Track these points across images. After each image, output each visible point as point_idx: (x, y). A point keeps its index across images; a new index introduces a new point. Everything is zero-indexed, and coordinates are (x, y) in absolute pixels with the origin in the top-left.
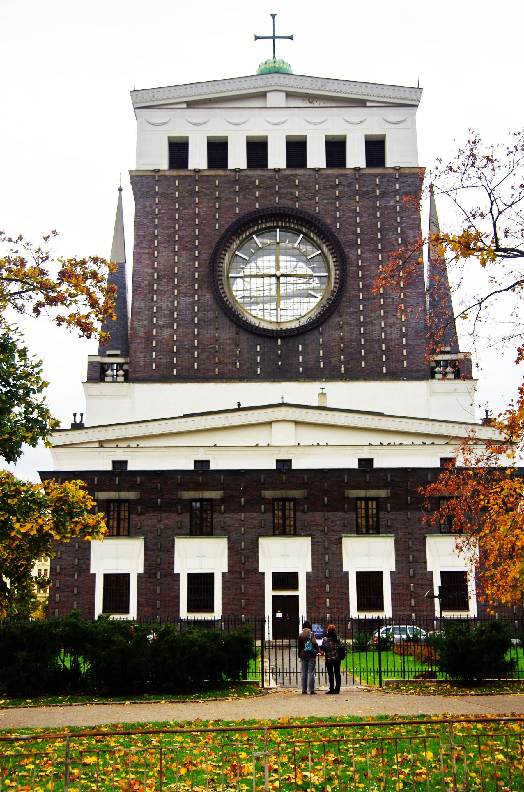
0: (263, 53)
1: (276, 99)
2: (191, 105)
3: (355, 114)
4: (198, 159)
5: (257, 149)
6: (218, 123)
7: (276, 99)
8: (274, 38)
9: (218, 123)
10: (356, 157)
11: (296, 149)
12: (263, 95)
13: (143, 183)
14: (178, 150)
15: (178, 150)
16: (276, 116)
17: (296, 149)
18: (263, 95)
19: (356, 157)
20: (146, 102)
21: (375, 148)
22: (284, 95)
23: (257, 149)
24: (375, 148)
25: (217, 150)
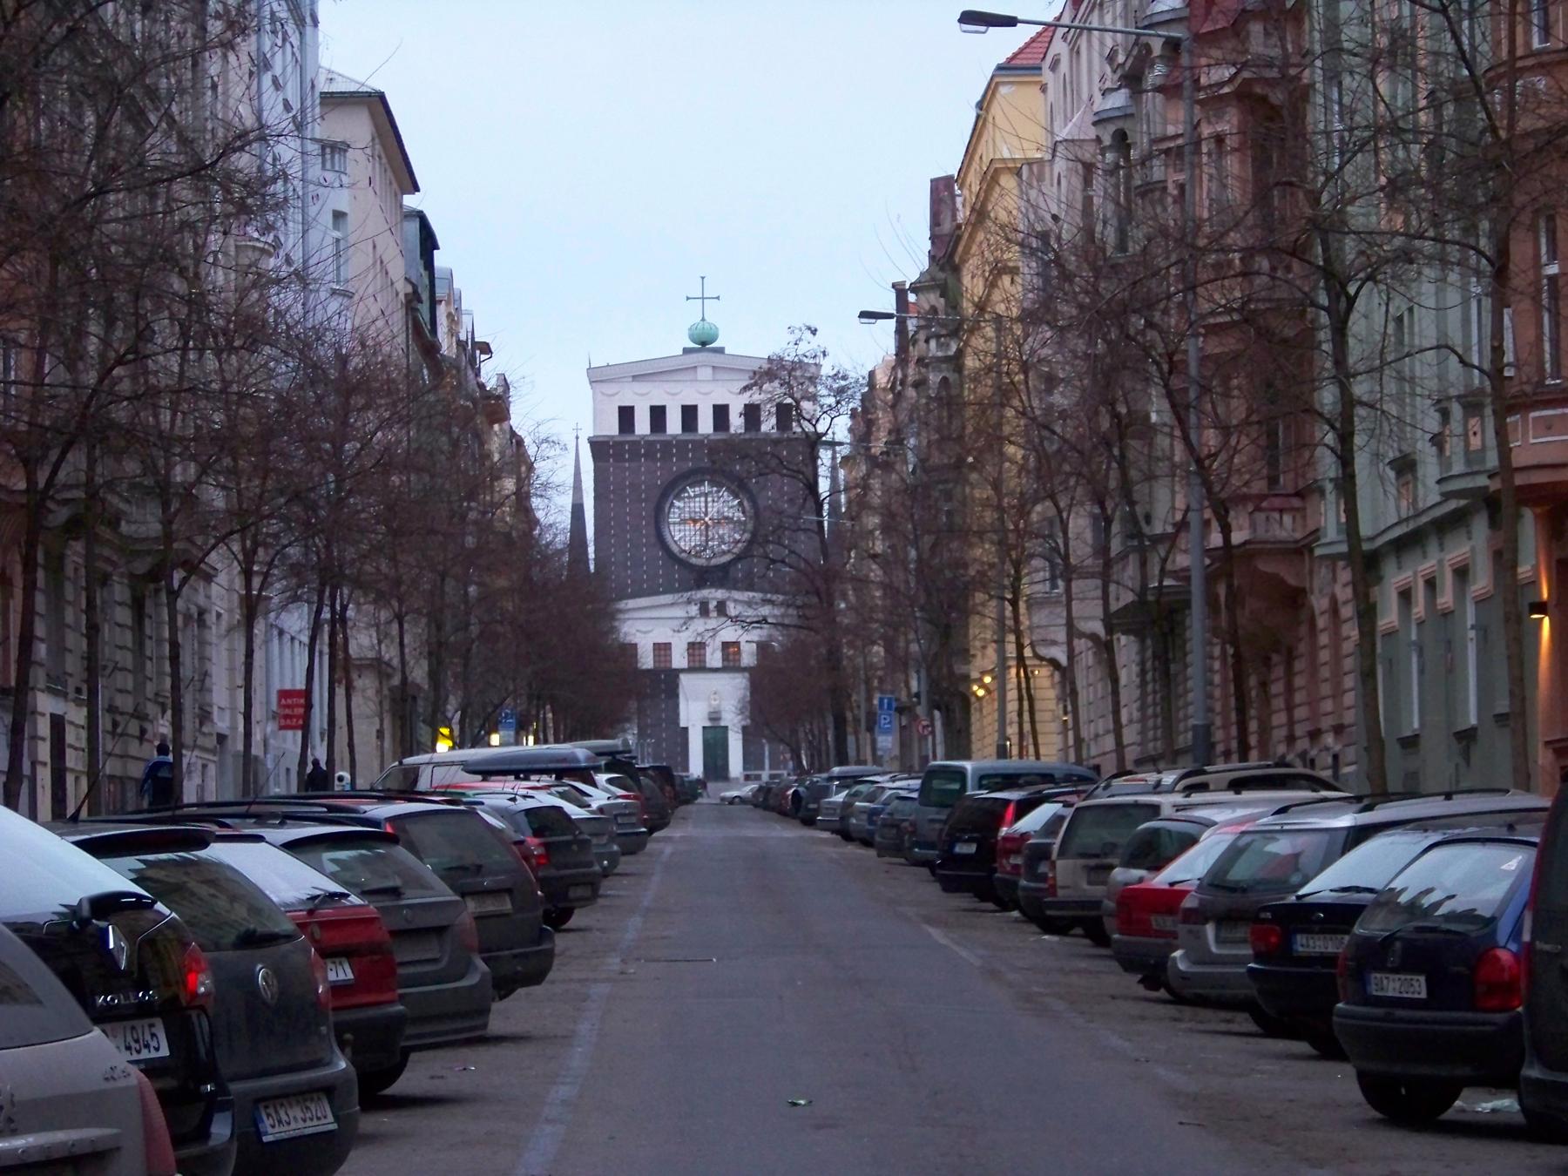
0: (690, 316)
1: (705, 373)
2: (635, 378)
4: (642, 426)
5: (690, 414)
7: (705, 373)
9: (657, 394)
13: (599, 447)
14: (626, 414)
15: (626, 414)
16: (706, 388)
20: (599, 377)
21: (785, 414)
22: (709, 370)
23: (690, 414)
25: (658, 414)
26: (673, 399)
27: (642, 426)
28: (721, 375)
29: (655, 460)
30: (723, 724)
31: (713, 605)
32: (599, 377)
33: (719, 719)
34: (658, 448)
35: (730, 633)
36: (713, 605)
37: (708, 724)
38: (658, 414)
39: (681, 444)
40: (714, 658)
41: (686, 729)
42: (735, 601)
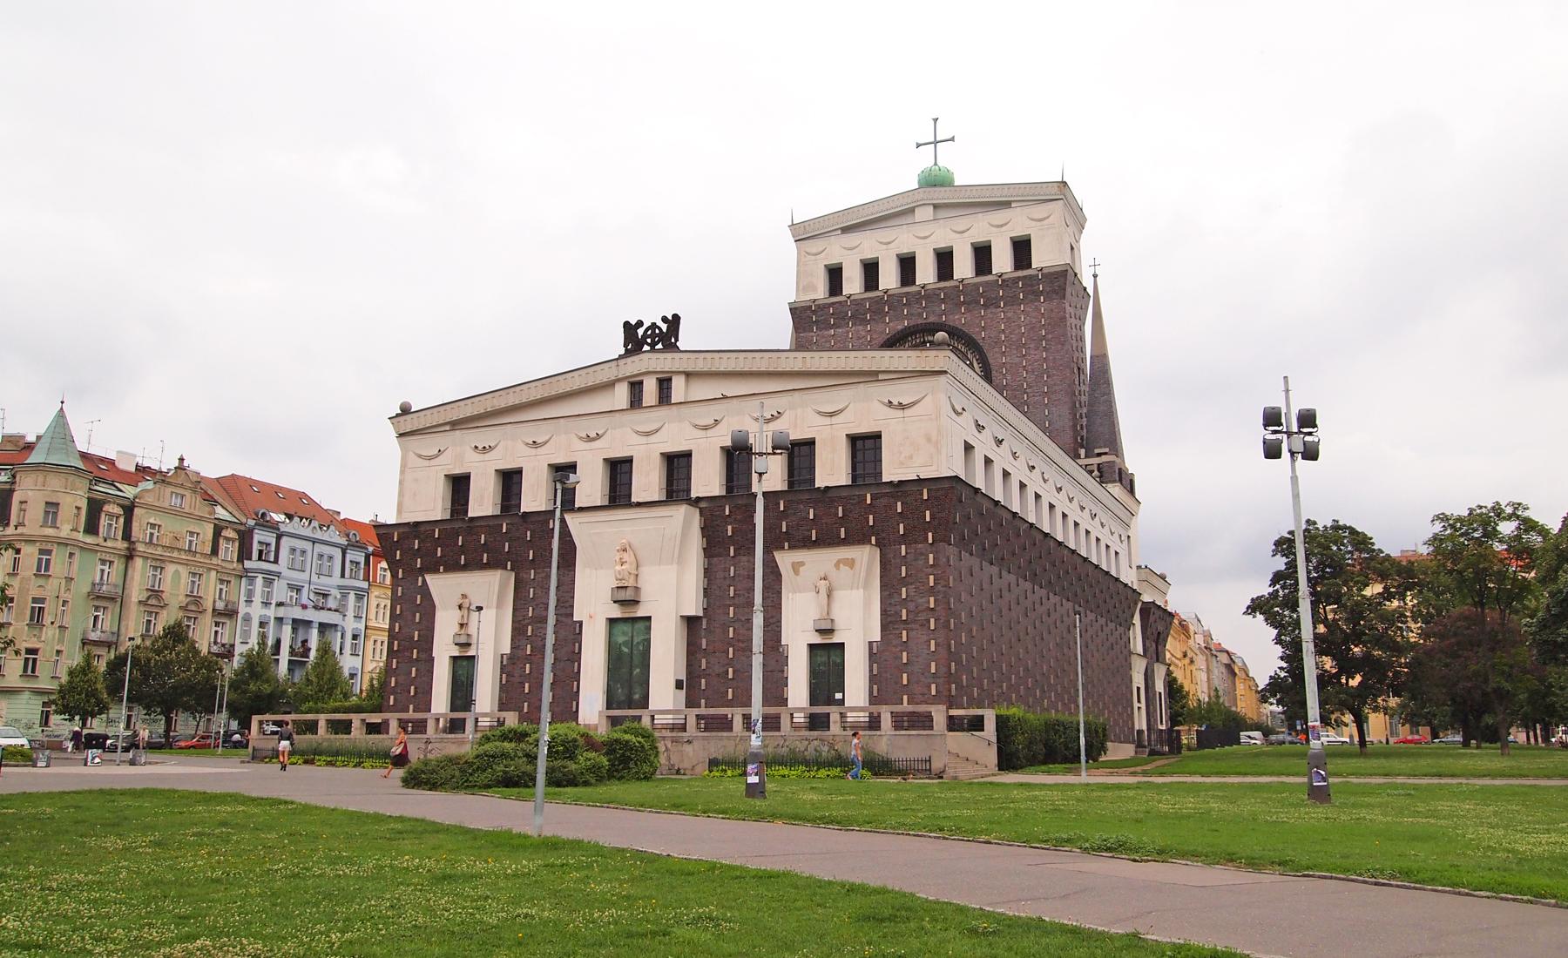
0: (924, 160)
1: (925, 213)
2: (845, 230)
3: (999, 216)
4: (853, 284)
5: (907, 265)
6: (869, 245)
7: (925, 213)
8: (936, 143)
9: (869, 245)
10: (1002, 261)
11: (944, 259)
12: (912, 210)
14: (835, 275)
15: (835, 275)
17: (944, 259)
18: (912, 210)
19: (1002, 261)
20: (805, 234)
21: (1022, 249)
24: (1022, 249)
26: (885, 247)
27: (853, 284)
28: (942, 213)
29: (865, 322)
30: (641, 612)
31: (650, 388)
32: (805, 234)
33: (635, 602)
34: (873, 307)
35: (675, 433)
36: (650, 388)
37: (616, 612)
38: (871, 270)
39: (892, 300)
40: (647, 482)
41: (581, 623)
42: (688, 375)
